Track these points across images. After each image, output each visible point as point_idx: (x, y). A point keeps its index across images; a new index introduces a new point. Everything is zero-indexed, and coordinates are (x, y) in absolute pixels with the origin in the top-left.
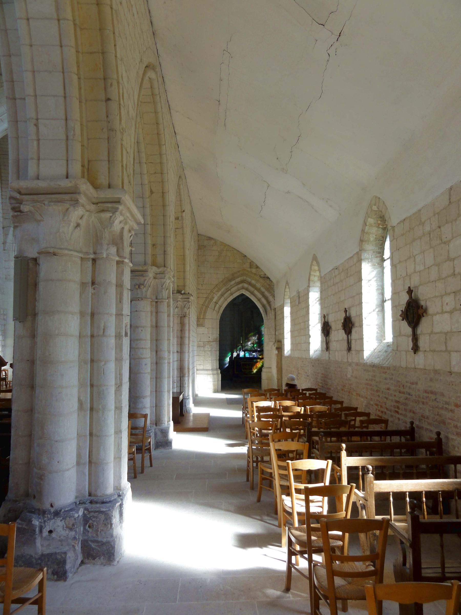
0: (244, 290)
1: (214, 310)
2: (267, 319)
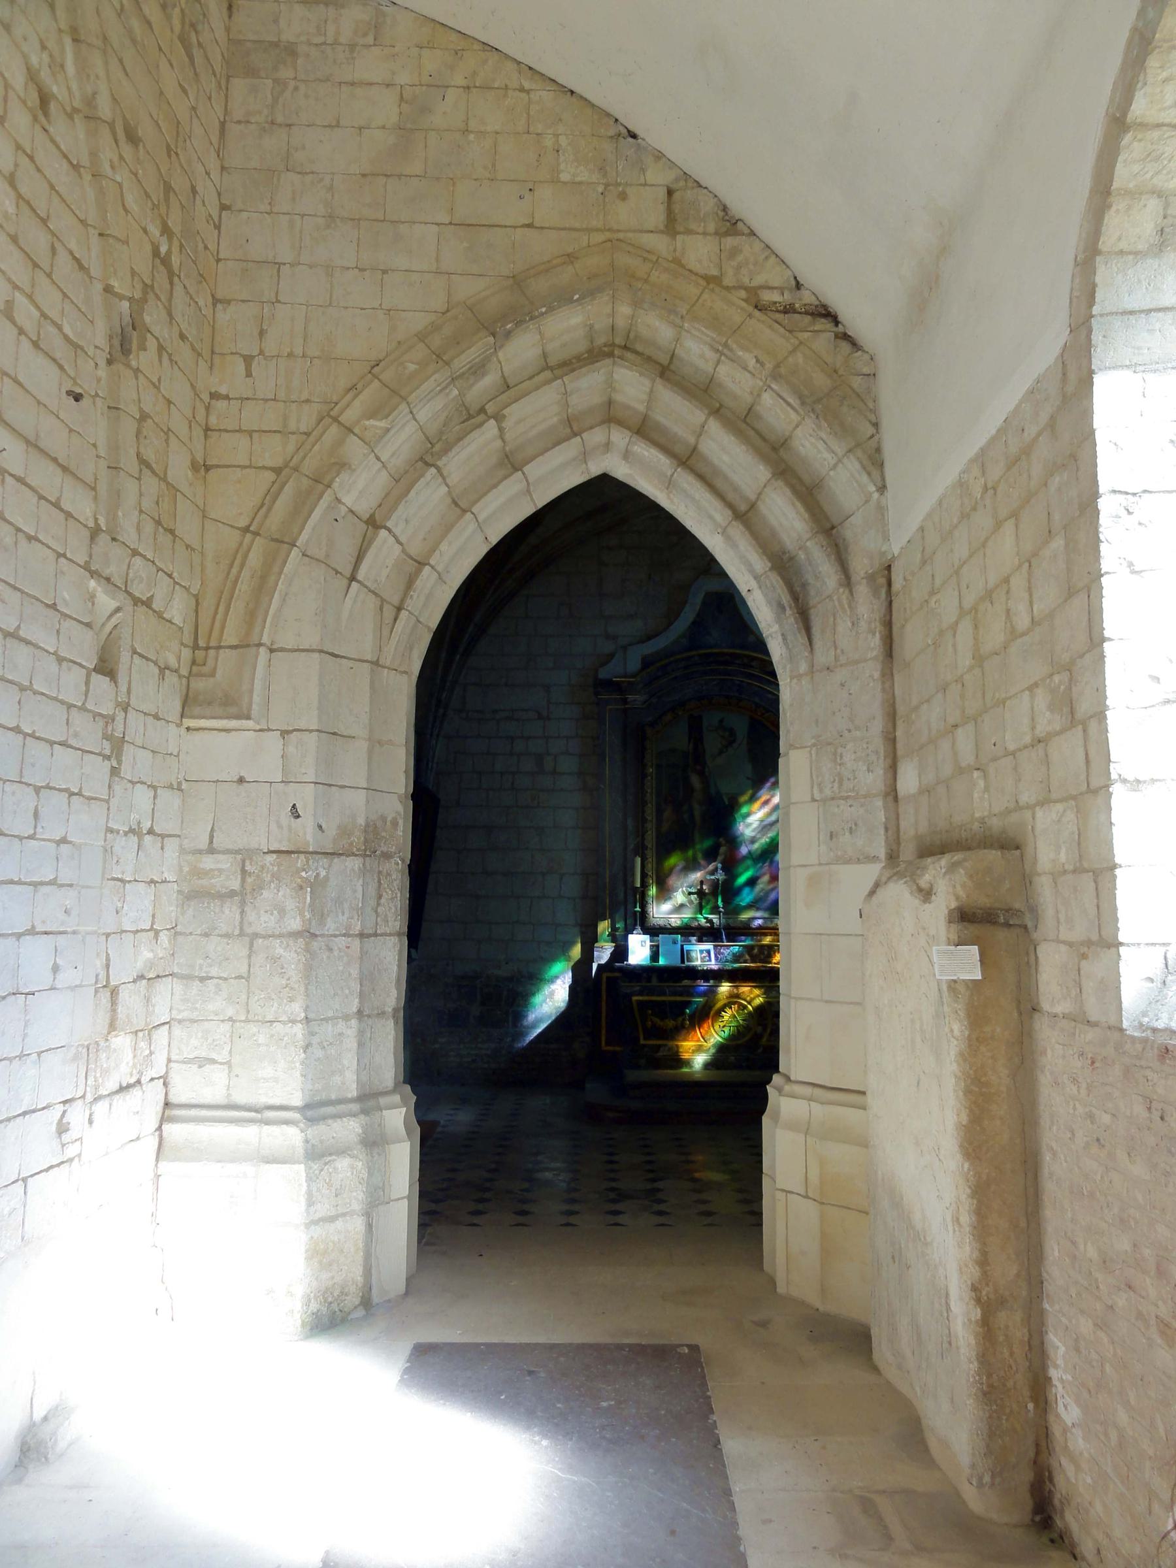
0: (620, 437)
1: (353, 578)
2: (812, 670)
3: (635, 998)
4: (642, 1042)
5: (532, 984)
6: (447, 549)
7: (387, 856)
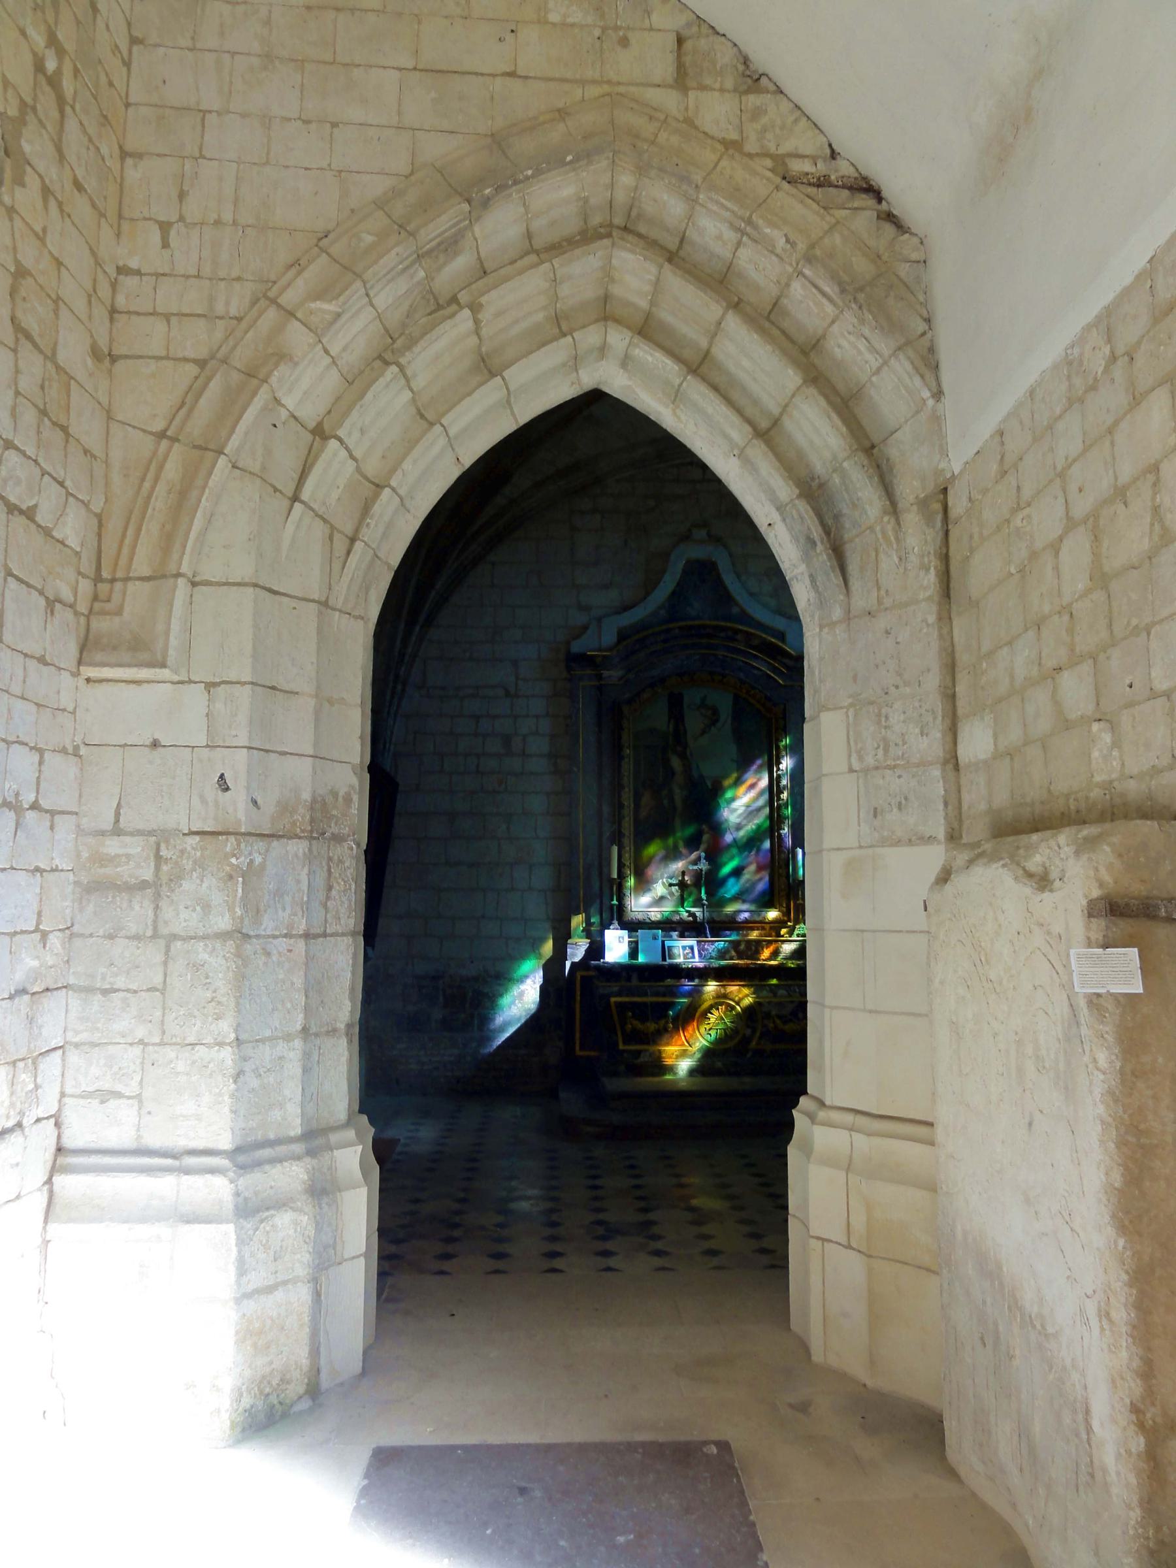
0: (618, 339)
1: (295, 498)
2: (848, 617)
3: (613, 1000)
4: (621, 1047)
5: (500, 985)
6: (411, 468)
7: (338, 839)
